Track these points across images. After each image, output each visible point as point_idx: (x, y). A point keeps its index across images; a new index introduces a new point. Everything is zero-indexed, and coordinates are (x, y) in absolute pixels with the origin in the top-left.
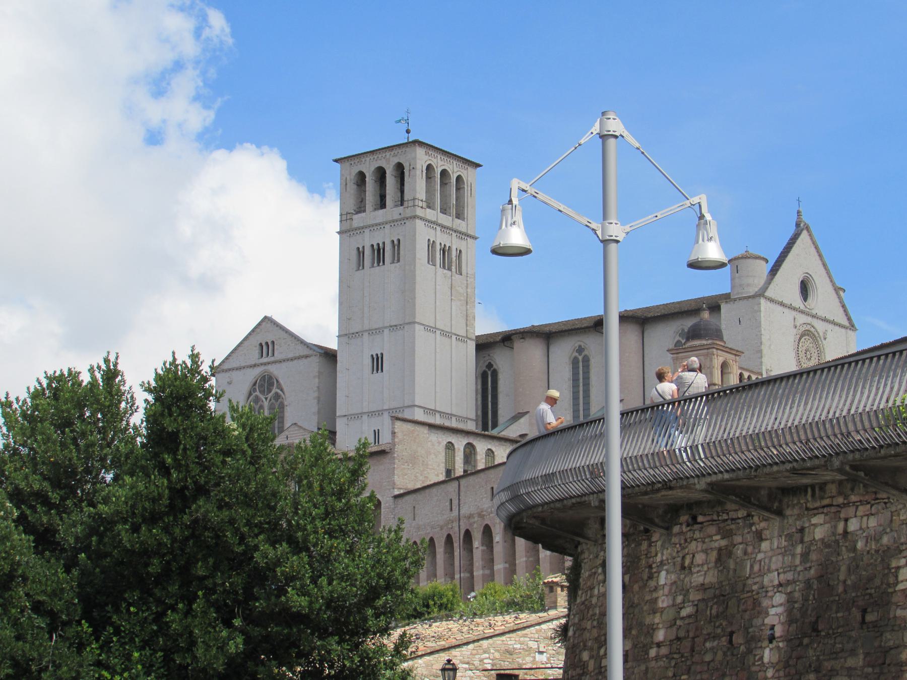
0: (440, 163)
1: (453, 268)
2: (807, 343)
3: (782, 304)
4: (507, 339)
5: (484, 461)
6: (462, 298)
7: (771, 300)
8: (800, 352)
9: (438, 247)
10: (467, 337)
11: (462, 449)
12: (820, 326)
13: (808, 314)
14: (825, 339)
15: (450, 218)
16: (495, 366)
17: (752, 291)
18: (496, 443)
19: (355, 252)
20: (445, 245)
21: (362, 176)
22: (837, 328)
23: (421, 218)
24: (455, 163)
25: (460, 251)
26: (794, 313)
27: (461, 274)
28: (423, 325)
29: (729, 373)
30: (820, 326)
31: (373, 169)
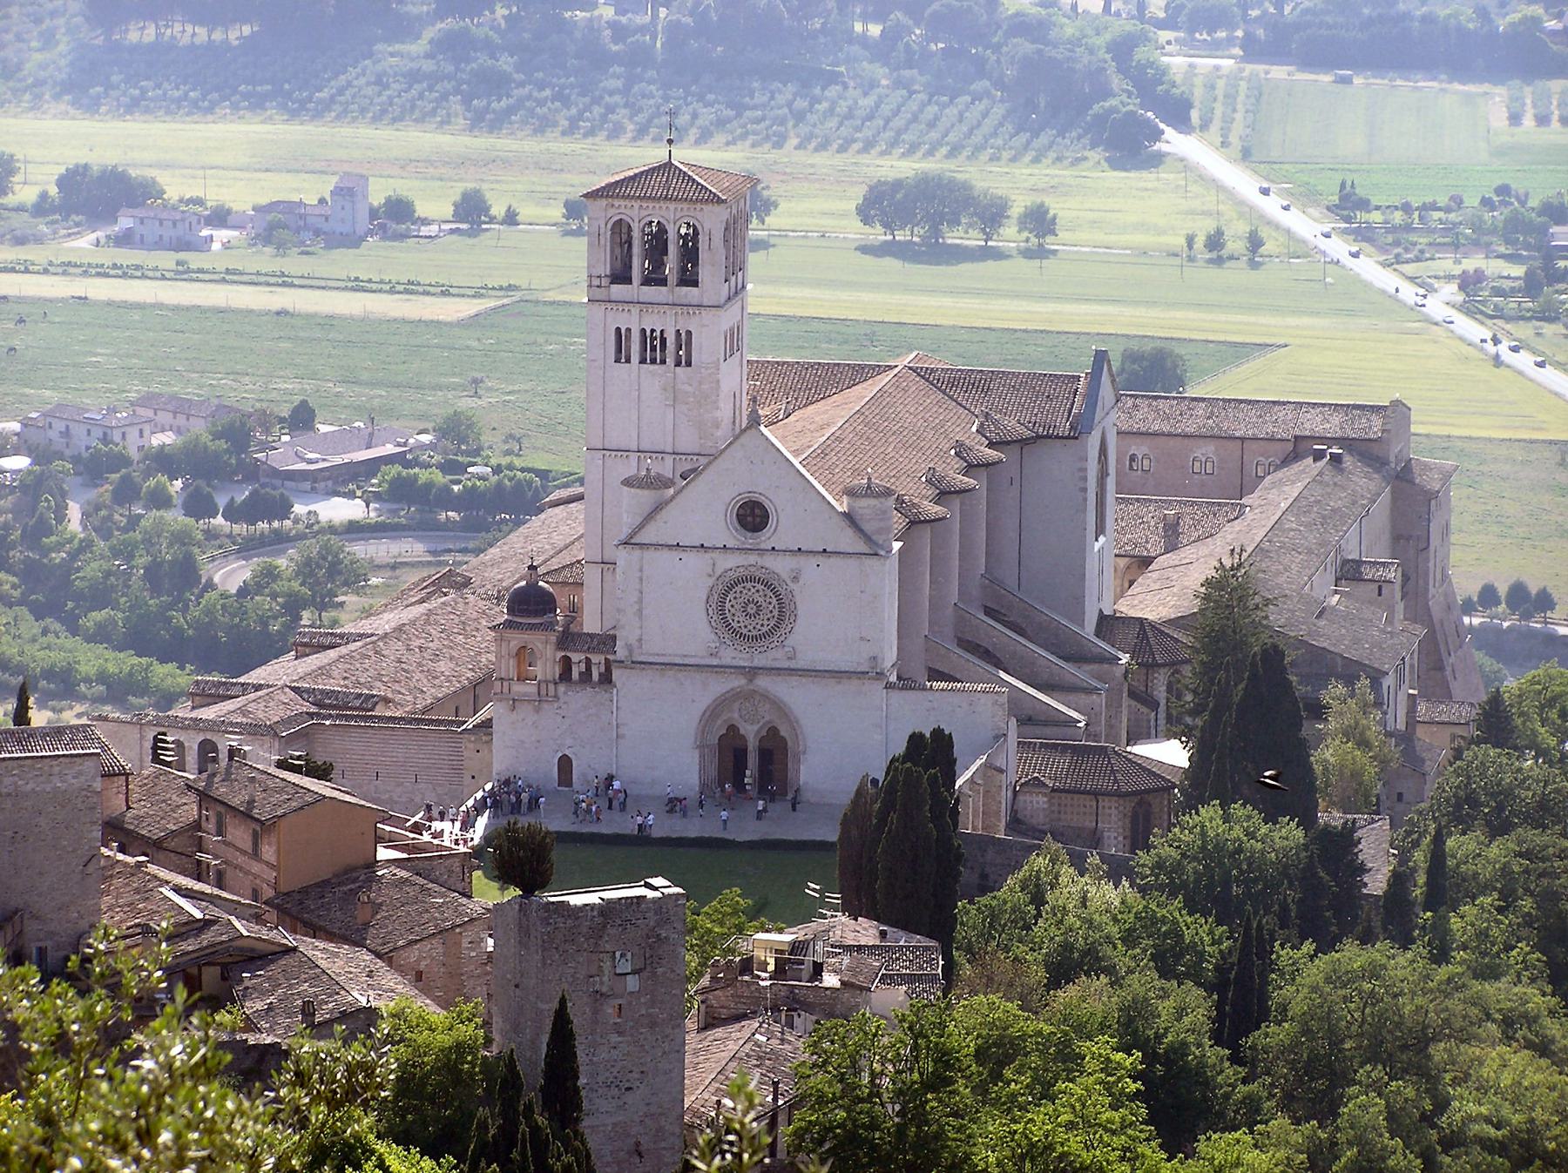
1: (670, 361)
7: (641, 545)
11: (196, 747)
22: (833, 560)
25: (689, 333)
26: (708, 556)
27: (689, 364)
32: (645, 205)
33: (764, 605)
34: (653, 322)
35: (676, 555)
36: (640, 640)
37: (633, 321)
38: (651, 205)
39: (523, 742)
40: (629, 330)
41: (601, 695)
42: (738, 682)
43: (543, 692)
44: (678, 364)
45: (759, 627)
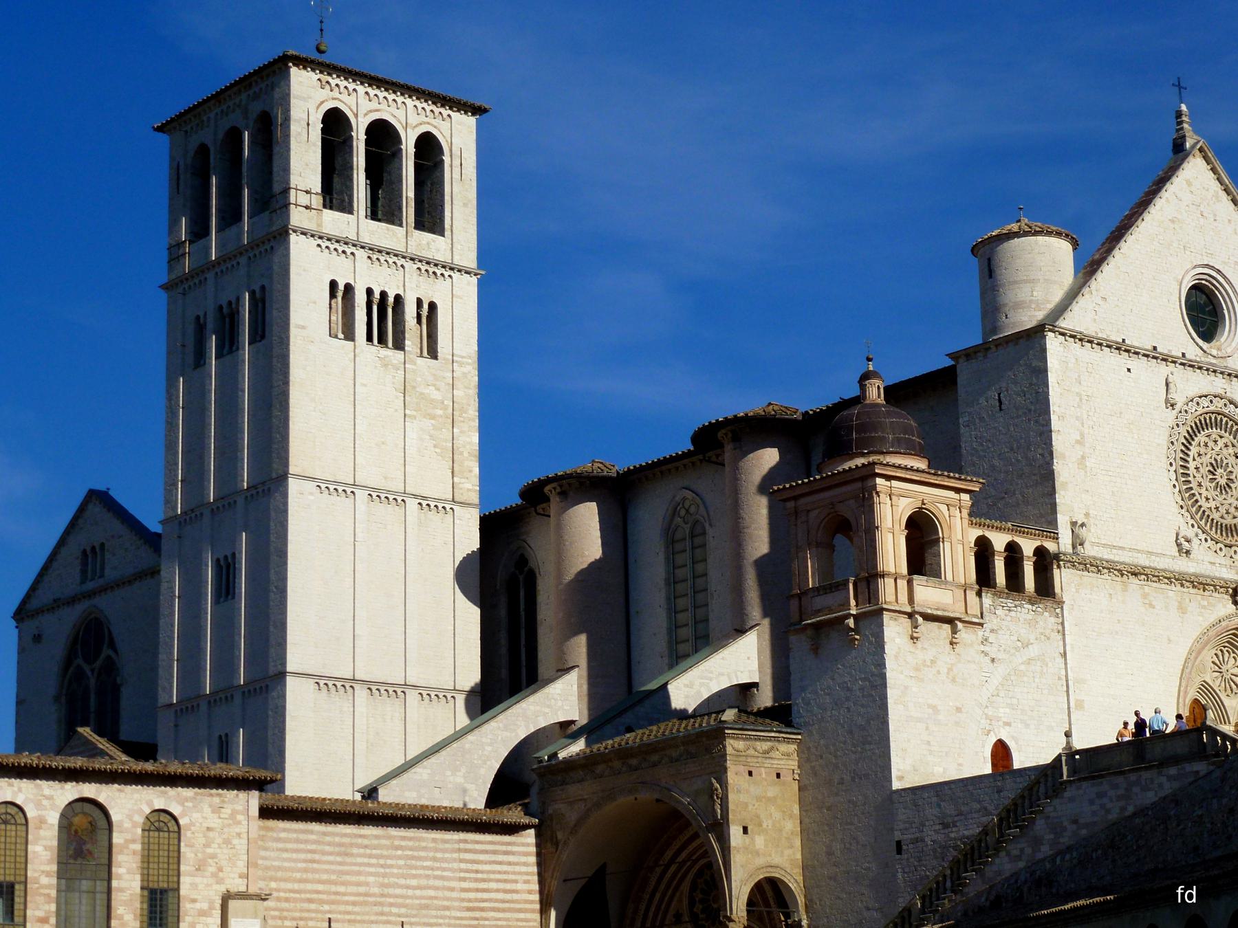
0: (365, 105)
3: (1120, 347)
4: (535, 495)
5: (138, 847)
6: (440, 412)
8: (1192, 471)
9: (360, 299)
10: (453, 501)
11: (54, 818)
15: (399, 231)
16: (532, 564)
17: (1026, 319)
19: (191, 329)
20: (384, 295)
21: (203, 150)
25: (433, 306)
26: (1164, 370)
28: (313, 479)
31: (221, 136)
34: (386, 280)
35: (1123, 360)
36: (1087, 515)
40: (349, 288)
41: (1045, 618)
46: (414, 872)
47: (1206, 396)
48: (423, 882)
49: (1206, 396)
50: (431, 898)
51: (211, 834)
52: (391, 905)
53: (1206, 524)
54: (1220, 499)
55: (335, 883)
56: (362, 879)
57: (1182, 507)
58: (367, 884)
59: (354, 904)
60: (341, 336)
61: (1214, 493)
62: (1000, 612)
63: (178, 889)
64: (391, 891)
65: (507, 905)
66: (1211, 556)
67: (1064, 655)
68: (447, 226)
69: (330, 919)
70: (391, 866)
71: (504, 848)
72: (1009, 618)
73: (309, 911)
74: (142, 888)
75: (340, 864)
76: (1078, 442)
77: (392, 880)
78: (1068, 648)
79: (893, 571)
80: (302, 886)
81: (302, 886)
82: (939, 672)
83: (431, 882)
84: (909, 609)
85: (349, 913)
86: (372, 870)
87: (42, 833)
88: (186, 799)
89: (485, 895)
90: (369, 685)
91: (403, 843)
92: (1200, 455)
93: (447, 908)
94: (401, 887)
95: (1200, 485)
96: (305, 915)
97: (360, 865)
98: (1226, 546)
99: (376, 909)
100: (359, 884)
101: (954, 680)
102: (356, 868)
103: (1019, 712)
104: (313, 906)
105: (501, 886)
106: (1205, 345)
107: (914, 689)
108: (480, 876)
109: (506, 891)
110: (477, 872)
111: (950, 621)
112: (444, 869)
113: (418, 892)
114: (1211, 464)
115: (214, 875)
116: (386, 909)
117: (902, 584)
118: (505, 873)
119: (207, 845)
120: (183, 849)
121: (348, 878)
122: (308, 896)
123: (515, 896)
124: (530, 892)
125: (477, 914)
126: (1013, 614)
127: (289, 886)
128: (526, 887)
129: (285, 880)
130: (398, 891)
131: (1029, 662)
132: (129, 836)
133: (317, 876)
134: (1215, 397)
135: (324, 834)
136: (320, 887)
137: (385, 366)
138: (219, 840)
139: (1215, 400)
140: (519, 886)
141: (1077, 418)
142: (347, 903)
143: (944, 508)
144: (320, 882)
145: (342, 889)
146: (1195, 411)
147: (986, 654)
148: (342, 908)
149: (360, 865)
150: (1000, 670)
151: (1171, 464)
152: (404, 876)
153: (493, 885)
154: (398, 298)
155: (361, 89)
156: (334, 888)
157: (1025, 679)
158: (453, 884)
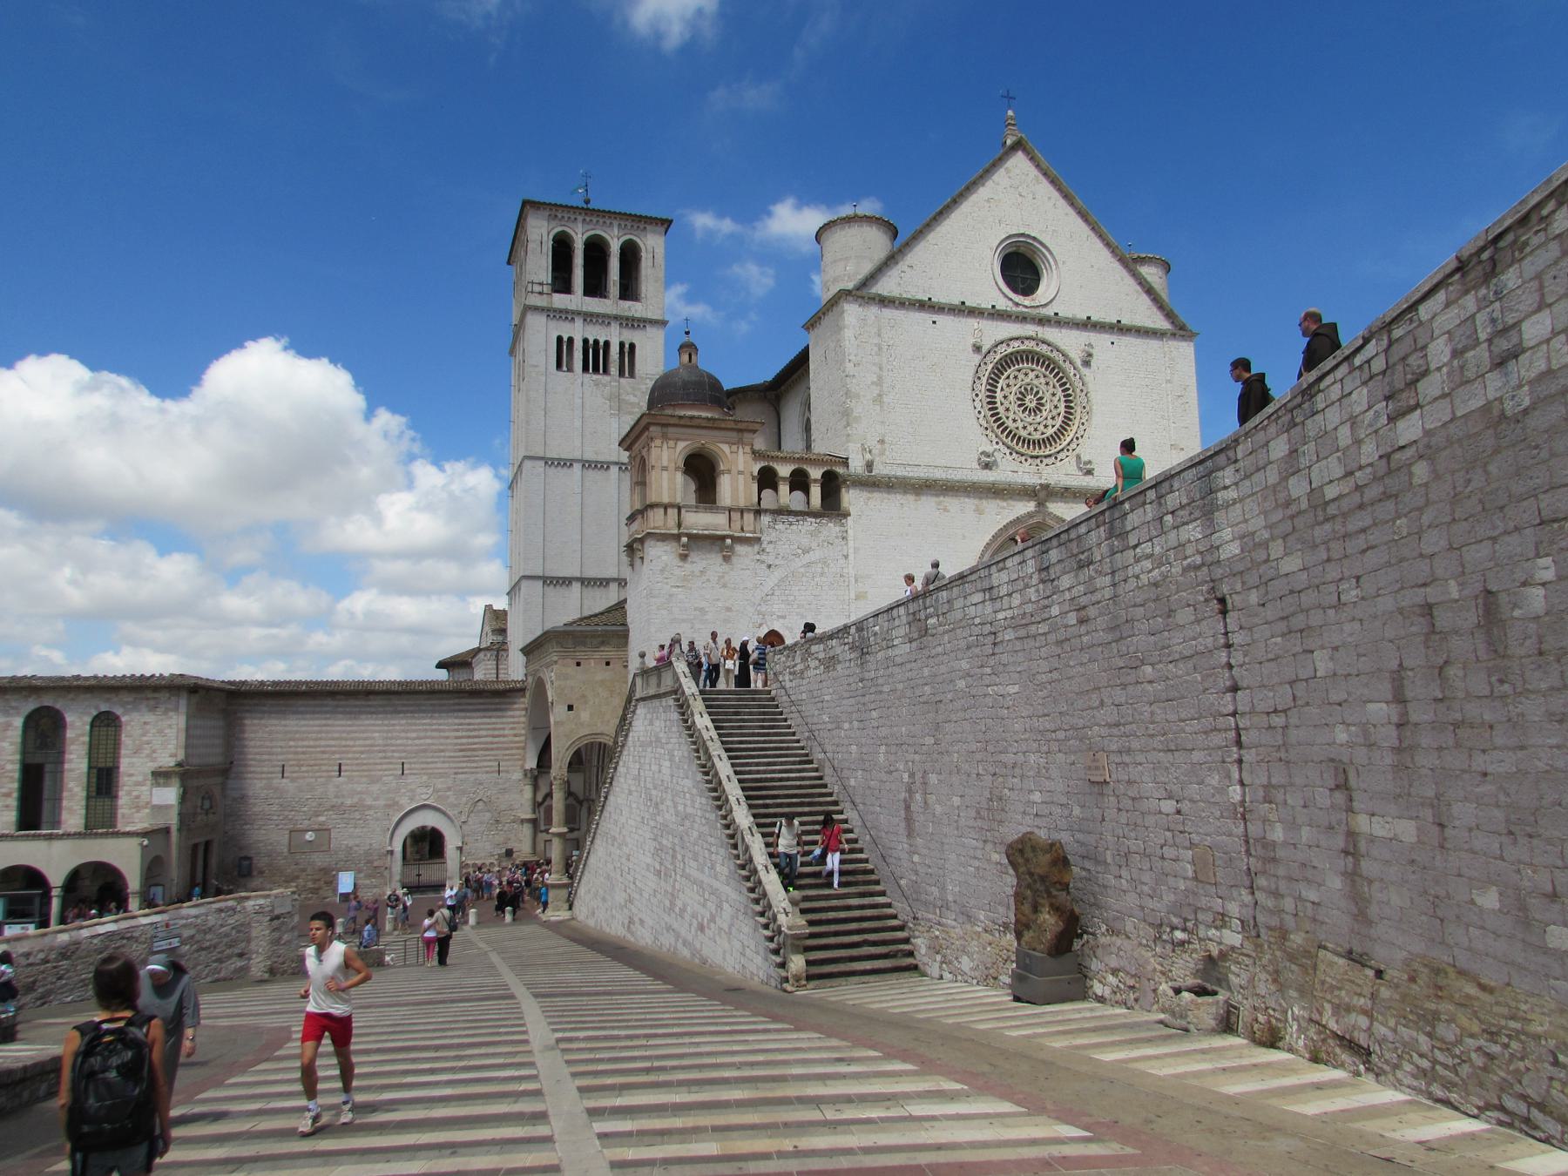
1: (614, 369)
2: (1030, 375)
5: (87, 739)
7: (884, 301)
9: (578, 345)
12: (1070, 342)
13: (1022, 319)
14: (1087, 363)
18: (127, 697)
20: (596, 342)
23: (536, 309)
24: (616, 223)
25: (632, 346)
26: (973, 323)
27: (632, 375)
29: (723, 472)
30: (1070, 342)
32: (588, 219)
33: (1047, 396)
34: (597, 333)
36: (882, 442)
37: (578, 332)
38: (595, 220)
39: (702, 610)
40: (571, 340)
41: (831, 528)
42: (1025, 507)
43: (737, 525)
44: (621, 374)
45: (1041, 428)
46: (414, 728)
47: (1017, 339)
48: (422, 734)
49: (1017, 339)
50: (429, 745)
51: (148, 727)
52: (393, 751)
53: (1012, 441)
54: (1029, 420)
55: (341, 739)
56: (369, 735)
57: (987, 429)
58: (374, 738)
59: (362, 753)
60: (565, 368)
61: (1022, 416)
62: (779, 526)
63: (118, 768)
64: (393, 742)
65: (495, 746)
66: (1015, 466)
67: (846, 557)
68: (643, 295)
69: (340, 765)
70: (393, 725)
71: (493, 707)
72: (789, 531)
73: (322, 759)
74: (90, 768)
75: (350, 726)
76: (873, 383)
77: (394, 734)
78: (851, 551)
79: (666, 500)
80: (318, 743)
81: (318, 743)
82: (708, 580)
83: (429, 734)
84: (676, 532)
85: (357, 759)
86: (377, 728)
87: (9, 733)
88: (128, 703)
89: (476, 740)
90: (577, 579)
91: (405, 709)
92: (1008, 386)
93: (443, 751)
94: (402, 738)
95: (1007, 410)
96: (318, 762)
97: (369, 725)
98: (1032, 457)
99: (380, 755)
100: (366, 739)
101: (724, 586)
102: (362, 728)
103: (795, 606)
104: (326, 756)
105: (491, 732)
106: (1018, 298)
107: (679, 596)
108: (472, 727)
109: (494, 736)
110: (469, 724)
111: (723, 538)
112: (440, 725)
113: (417, 742)
114: (1020, 393)
115: (148, 756)
116: (390, 754)
117: (676, 511)
118: (494, 723)
119: (144, 735)
120: (123, 737)
121: (357, 735)
122: (323, 749)
123: (501, 739)
124: (515, 735)
125: (469, 753)
126: (794, 527)
127: (306, 743)
128: (512, 732)
129: (303, 740)
130: (399, 742)
131: (809, 565)
132: (79, 732)
133: (330, 735)
134: (1027, 339)
135: (337, 706)
136: (333, 743)
137: (597, 385)
138: (154, 731)
139: (1026, 342)
140: (506, 732)
141: (874, 364)
142: (354, 752)
143: (725, 448)
144: (333, 739)
145: (351, 743)
146: (1003, 350)
147: (763, 562)
148: (350, 756)
149: (369, 725)
150: (777, 575)
151: (977, 395)
152: (407, 731)
153: (484, 733)
154: (607, 344)
155: (580, 218)
156: (344, 743)
157: (804, 579)
158: (447, 734)
